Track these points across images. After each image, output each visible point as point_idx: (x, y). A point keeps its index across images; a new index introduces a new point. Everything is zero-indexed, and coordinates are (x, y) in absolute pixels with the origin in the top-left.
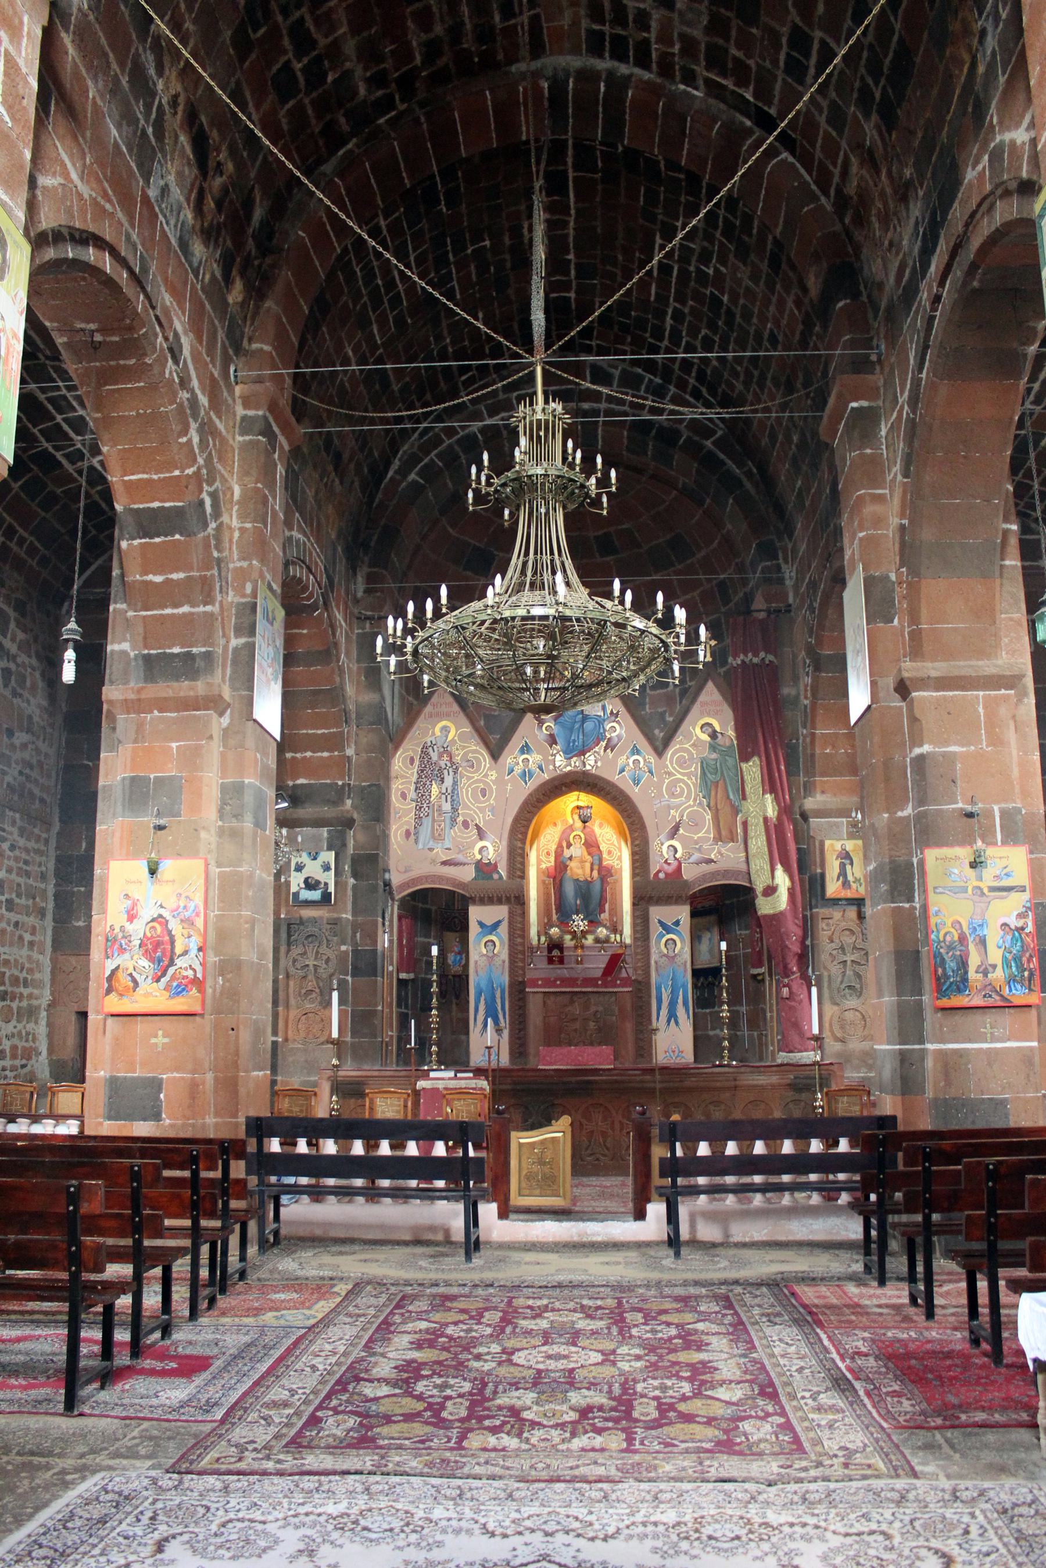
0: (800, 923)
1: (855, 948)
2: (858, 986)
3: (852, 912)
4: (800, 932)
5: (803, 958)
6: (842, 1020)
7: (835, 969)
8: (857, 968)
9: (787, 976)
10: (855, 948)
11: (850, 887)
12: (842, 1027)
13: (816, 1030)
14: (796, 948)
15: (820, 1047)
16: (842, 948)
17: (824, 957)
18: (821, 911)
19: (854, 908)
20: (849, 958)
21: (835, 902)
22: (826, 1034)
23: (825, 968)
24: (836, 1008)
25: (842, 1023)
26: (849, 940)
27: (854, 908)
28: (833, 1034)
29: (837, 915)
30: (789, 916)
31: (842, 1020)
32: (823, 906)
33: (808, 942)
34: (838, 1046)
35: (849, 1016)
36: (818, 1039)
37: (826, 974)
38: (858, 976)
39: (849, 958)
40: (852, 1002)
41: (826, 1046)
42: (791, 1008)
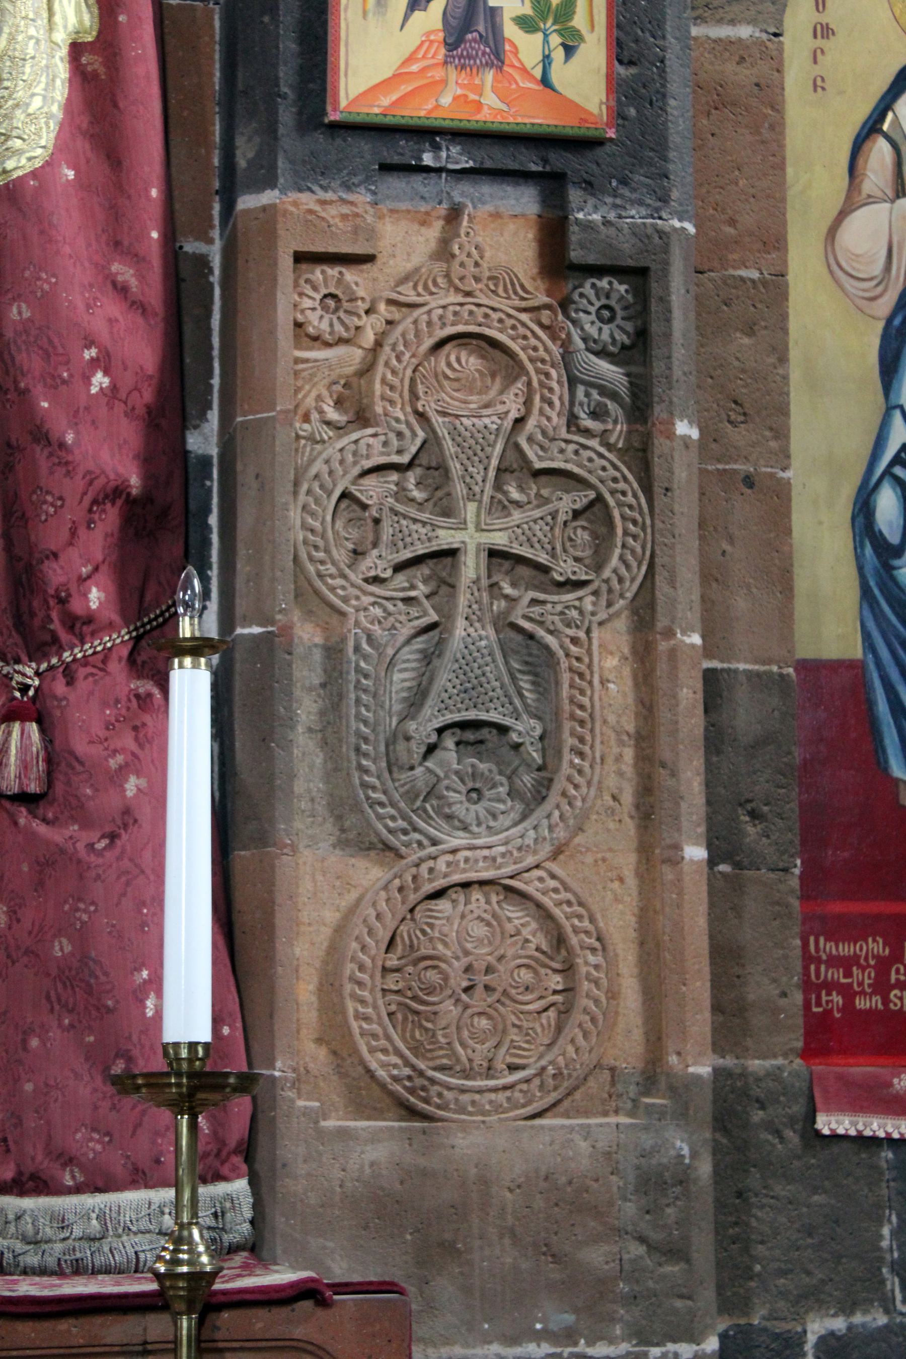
0: (147, 281)
1: (514, 466)
2: (526, 729)
3: (504, 230)
4: (143, 351)
5: (168, 522)
6: (405, 954)
7: (377, 618)
8: (523, 602)
9: (39, 646)
10: (514, 466)
11: (497, 53)
12: (412, 1010)
13: (187, 1008)
14: (111, 453)
15: (250, 1153)
16: (429, 464)
17: (298, 520)
18: (300, 208)
19: (524, 202)
20: (471, 535)
21: (396, 147)
22: (297, 1059)
23: (307, 595)
24: (370, 874)
25: (412, 984)
26: (476, 409)
27: (524, 202)
28: (335, 1035)
29: (403, 238)
30: (71, 233)
31: (405, 954)
32: (313, 172)
33: (204, 440)
34: (376, 1146)
35: (462, 928)
36: (199, 1082)
37: (308, 634)
38: (531, 655)
39: (471, 535)
40: (484, 839)
41: (292, 1148)
42: (49, 863)
